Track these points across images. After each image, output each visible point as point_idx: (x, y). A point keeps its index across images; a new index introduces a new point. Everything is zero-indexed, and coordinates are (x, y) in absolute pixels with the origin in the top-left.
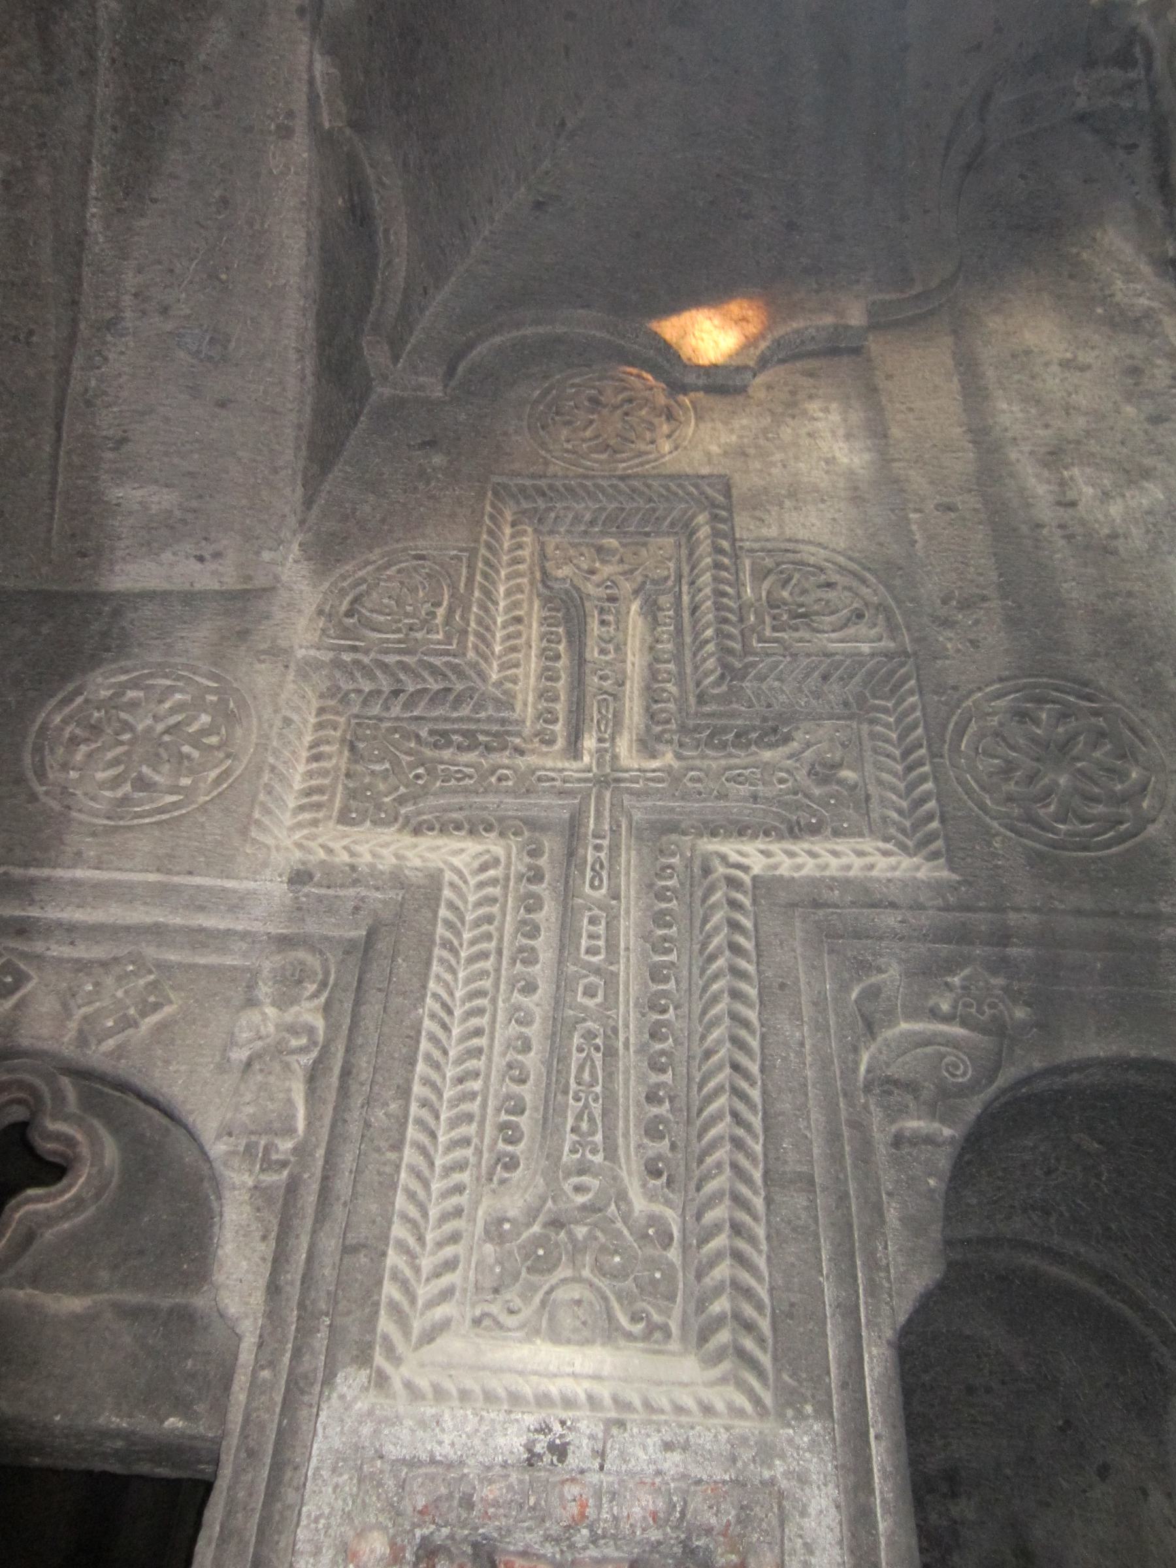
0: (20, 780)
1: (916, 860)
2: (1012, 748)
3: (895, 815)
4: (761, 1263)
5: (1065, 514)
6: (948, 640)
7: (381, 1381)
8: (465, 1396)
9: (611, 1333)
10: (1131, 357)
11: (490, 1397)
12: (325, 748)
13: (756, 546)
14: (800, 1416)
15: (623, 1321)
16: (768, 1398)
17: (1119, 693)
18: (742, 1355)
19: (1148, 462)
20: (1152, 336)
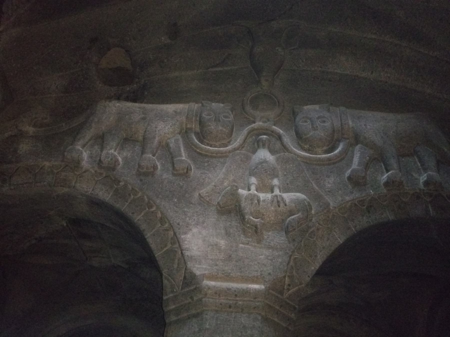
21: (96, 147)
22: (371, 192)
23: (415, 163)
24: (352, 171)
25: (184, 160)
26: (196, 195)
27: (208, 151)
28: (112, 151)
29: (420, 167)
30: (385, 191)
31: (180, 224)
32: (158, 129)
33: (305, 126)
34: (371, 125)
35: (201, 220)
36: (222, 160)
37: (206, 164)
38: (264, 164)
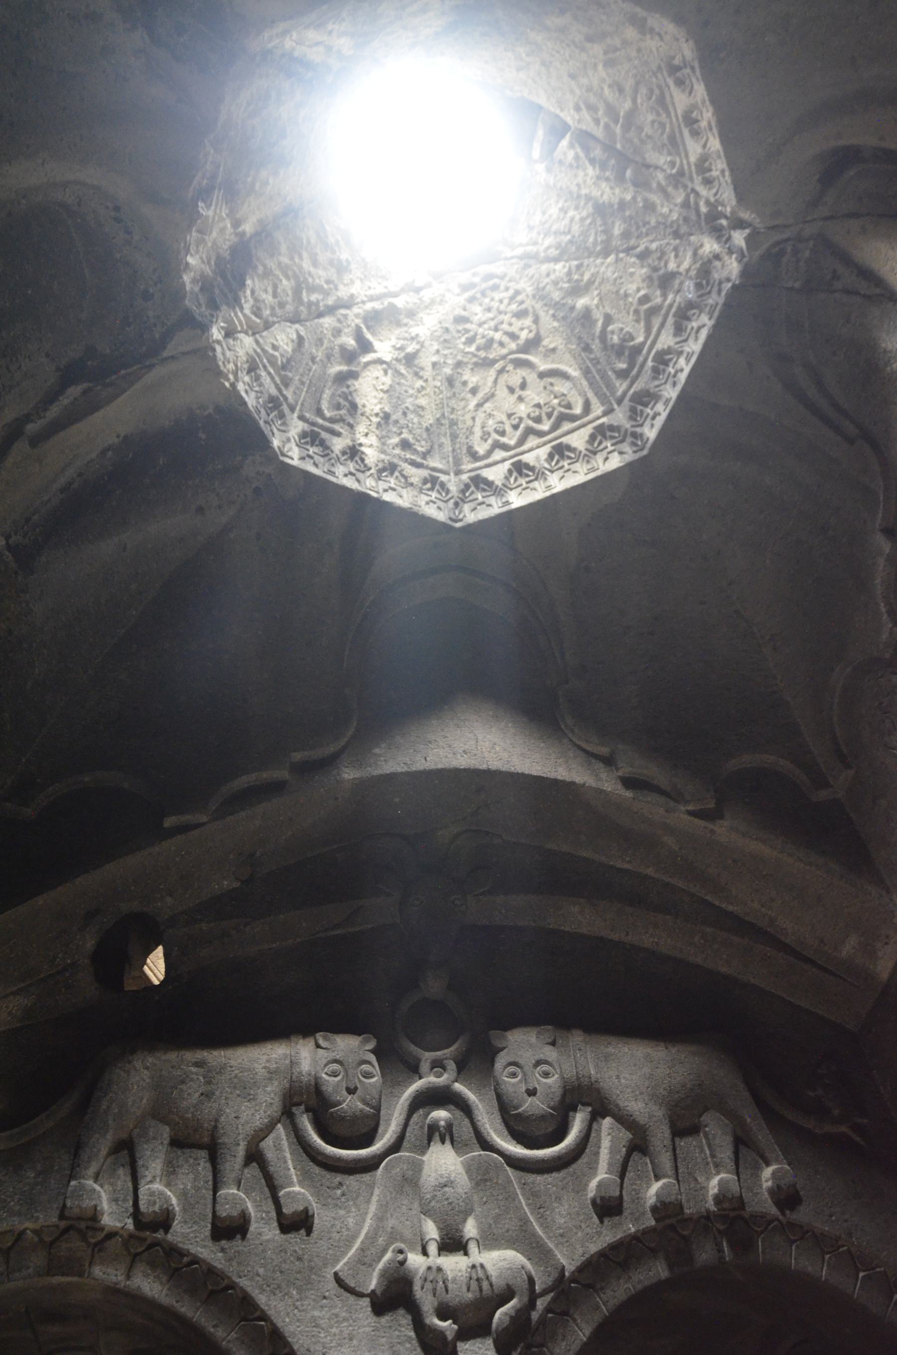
21: (121, 1172)
22: (630, 1229)
23: (702, 1151)
24: (600, 1185)
25: (299, 1193)
26: (330, 1276)
27: (340, 1159)
28: (157, 1186)
29: (709, 1160)
30: (653, 1223)
31: (312, 1349)
32: (242, 1121)
33: (512, 1084)
34: (627, 1076)
35: (346, 1332)
36: (366, 1177)
37: (339, 1192)
38: (446, 1189)
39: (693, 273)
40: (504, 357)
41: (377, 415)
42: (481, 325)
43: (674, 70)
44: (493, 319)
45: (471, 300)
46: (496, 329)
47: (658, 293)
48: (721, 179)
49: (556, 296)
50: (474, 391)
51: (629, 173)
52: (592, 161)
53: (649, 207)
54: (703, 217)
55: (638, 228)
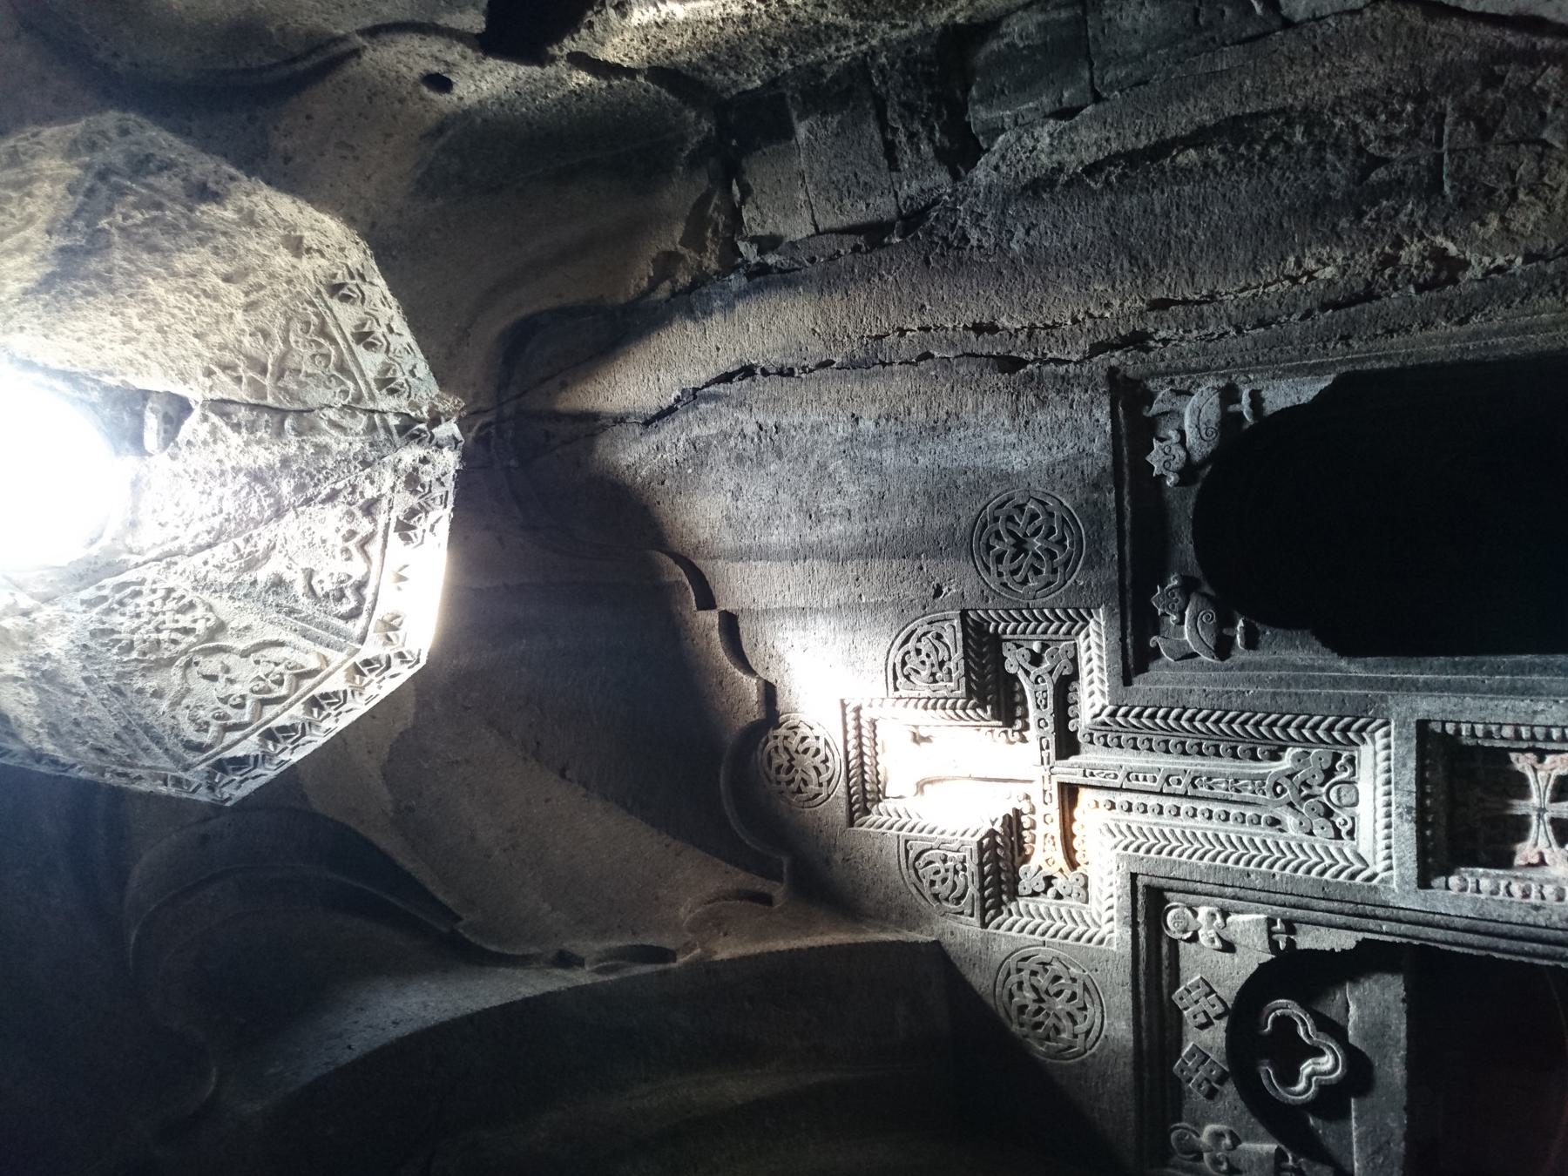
0: (1083, 1063)
1: (1092, 622)
2: (1020, 568)
3: (1064, 629)
4: (1316, 718)
5: (856, 517)
6: (950, 591)
7: (1382, 881)
8: (1388, 847)
9: (1350, 782)
10: (728, 459)
11: (1388, 837)
12: (1042, 910)
13: (891, 686)
14: (1388, 709)
15: (1345, 775)
16: (1379, 722)
17: (980, 507)
18: (1363, 728)
19: (813, 465)
20: (709, 444)
39: (400, 486)
40: (185, 652)
41: (40, 726)
42: (133, 632)
43: (335, 289)
44: (148, 623)
45: (110, 611)
46: (158, 630)
47: (365, 521)
48: (411, 380)
49: (227, 578)
50: (158, 694)
51: (288, 423)
52: (237, 427)
53: (322, 450)
54: (394, 431)
55: (312, 478)
